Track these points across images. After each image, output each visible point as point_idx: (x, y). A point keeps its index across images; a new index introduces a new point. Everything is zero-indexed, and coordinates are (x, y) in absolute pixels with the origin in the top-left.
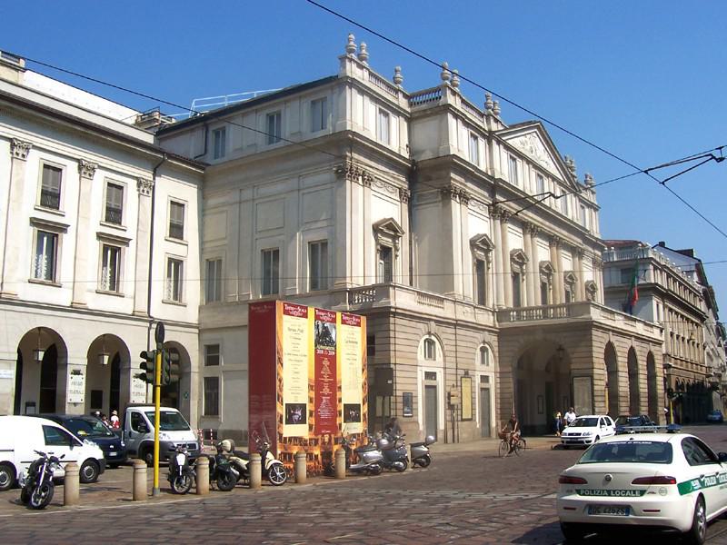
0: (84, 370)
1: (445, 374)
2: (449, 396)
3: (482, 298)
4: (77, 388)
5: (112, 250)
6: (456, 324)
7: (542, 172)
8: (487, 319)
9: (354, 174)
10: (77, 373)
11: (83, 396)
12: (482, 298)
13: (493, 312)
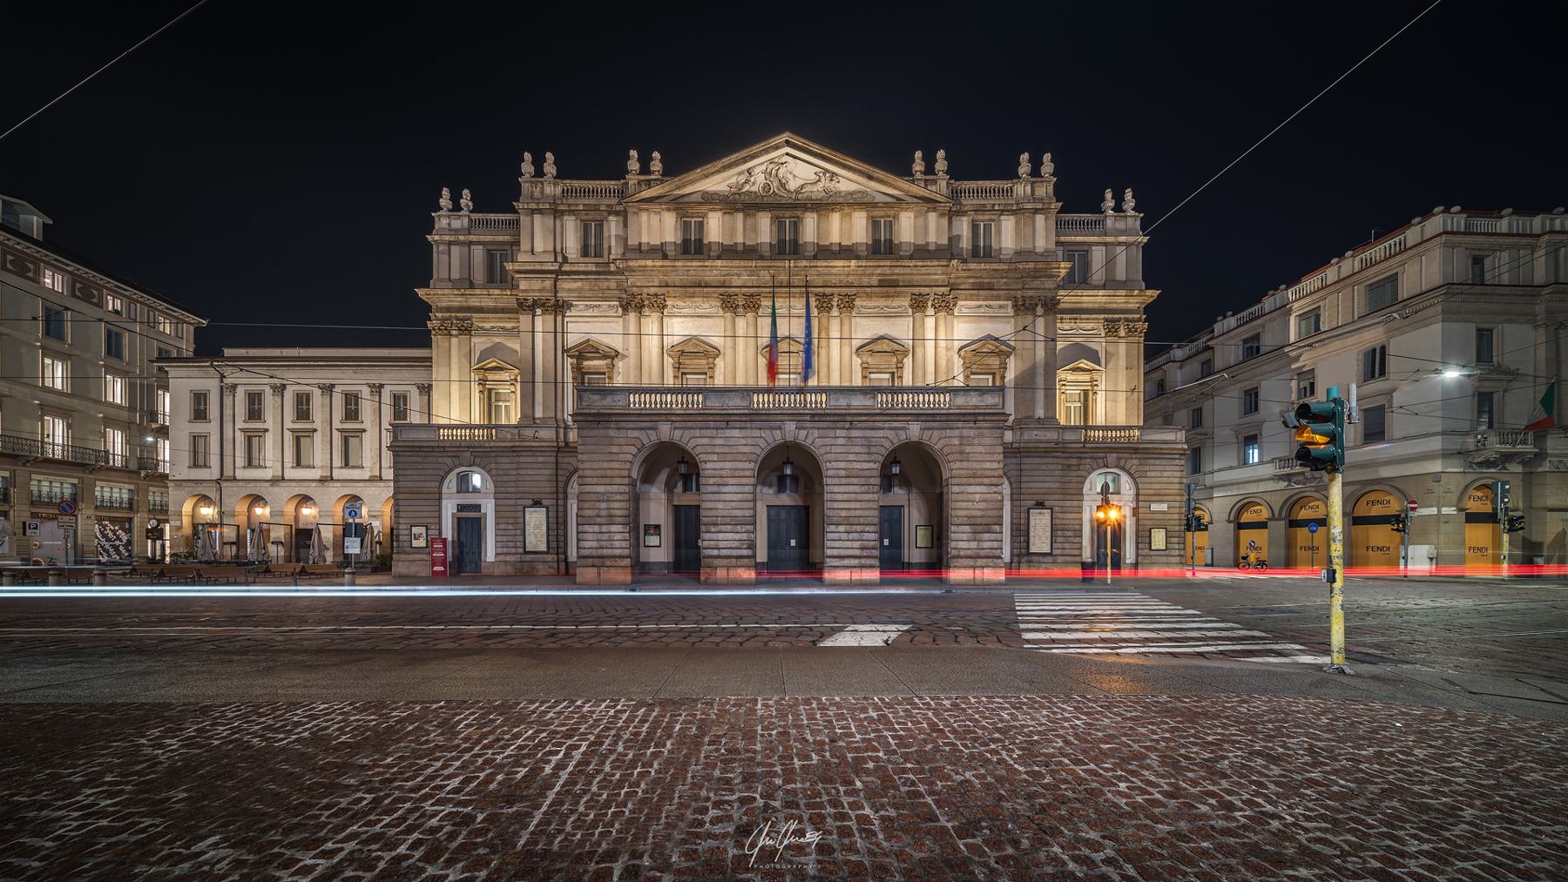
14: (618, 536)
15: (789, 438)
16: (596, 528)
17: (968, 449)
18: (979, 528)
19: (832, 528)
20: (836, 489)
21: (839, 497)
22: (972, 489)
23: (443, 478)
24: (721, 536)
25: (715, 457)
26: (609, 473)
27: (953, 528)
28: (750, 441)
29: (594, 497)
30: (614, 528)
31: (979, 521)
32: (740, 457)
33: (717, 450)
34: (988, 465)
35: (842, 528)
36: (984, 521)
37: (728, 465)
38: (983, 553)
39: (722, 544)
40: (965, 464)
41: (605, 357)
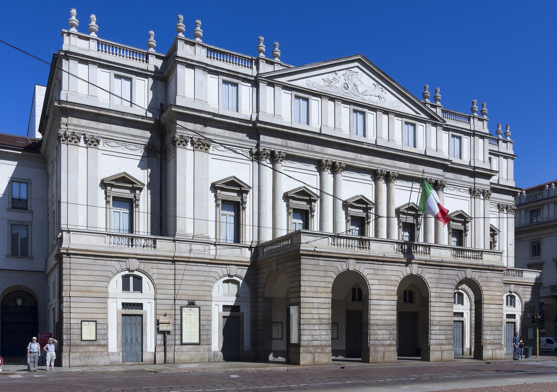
1: (156, 304)
2: (158, 323)
3: (237, 237)
12: (237, 237)
13: (250, 248)
15: (414, 273)
16: (311, 327)
17: (490, 284)
21: (436, 309)
22: (491, 306)
24: (380, 332)
25: (376, 282)
26: (320, 290)
28: (394, 273)
29: (310, 305)
30: (322, 327)
32: (389, 283)
36: (496, 324)
37: (384, 287)
40: (489, 293)
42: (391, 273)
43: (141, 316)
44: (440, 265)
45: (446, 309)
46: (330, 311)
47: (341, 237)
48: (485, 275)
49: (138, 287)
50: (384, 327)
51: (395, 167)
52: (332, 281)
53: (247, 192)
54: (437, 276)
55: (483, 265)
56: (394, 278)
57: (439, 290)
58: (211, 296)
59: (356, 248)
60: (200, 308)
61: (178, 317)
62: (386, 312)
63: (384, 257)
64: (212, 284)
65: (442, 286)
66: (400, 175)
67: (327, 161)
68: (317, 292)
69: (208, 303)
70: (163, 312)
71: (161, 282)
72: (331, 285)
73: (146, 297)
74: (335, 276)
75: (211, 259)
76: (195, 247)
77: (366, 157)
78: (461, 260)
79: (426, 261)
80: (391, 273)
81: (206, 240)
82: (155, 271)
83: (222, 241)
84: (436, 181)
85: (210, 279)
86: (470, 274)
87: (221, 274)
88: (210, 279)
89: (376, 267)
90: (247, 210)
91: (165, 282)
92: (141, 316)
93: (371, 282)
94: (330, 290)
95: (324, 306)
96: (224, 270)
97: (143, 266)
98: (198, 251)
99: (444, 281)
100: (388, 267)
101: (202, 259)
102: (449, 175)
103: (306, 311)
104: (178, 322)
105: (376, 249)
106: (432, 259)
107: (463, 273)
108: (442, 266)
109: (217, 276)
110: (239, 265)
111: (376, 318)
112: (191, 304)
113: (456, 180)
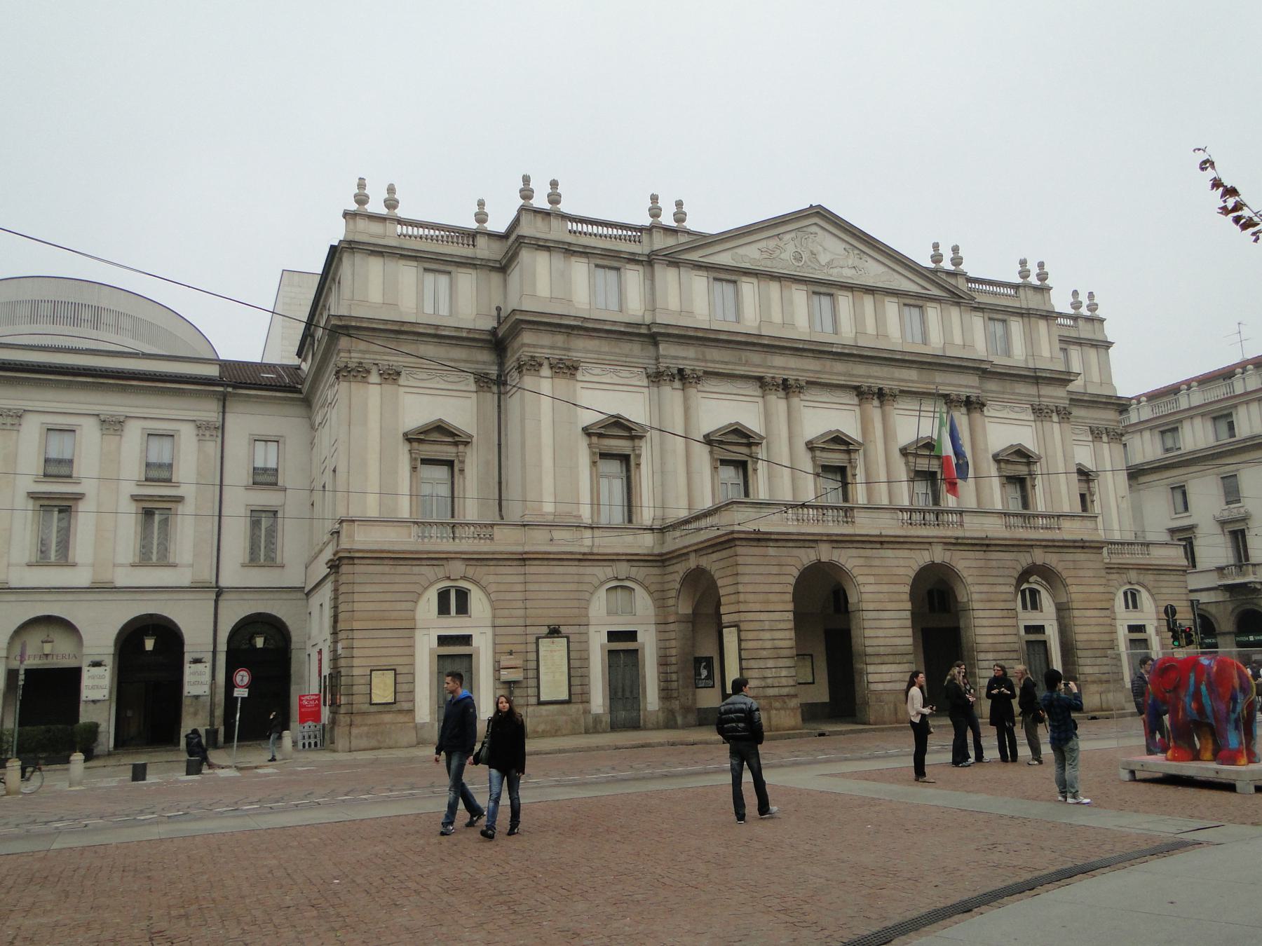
0: (109, 661)
1: (495, 635)
2: (497, 669)
4: (96, 682)
5: (154, 513)
6: (523, 559)
7: (824, 288)
8: (647, 543)
9: (358, 373)
10: (97, 664)
11: (106, 692)
14: (784, 673)
16: (761, 664)
17: (1081, 573)
18: (1098, 653)
19: (982, 656)
20: (980, 614)
21: (985, 622)
22: (1089, 613)
23: (420, 595)
24: (884, 668)
25: (871, 579)
27: (1079, 653)
28: (902, 562)
30: (781, 663)
31: (1097, 645)
33: (876, 571)
34: (1096, 589)
35: (990, 656)
36: (1100, 645)
37: (885, 588)
38: (1105, 677)
39: (886, 677)
40: (1081, 589)
41: (632, 438)
42: (895, 562)
43: (470, 656)
44: (984, 545)
45: (1003, 622)
46: (792, 634)
47: (808, 507)
48: (1069, 557)
49: (463, 609)
50: (891, 659)
51: (892, 379)
52: (793, 581)
53: (641, 437)
54: (982, 563)
55: (1064, 541)
56: (902, 571)
57: (984, 588)
58: (587, 616)
59: (831, 524)
60: (568, 638)
61: (532, 656)
62: (893, 632)
63: (881, 536)
64: (587, 596)
65: (991, 580)
66: (902, 391)
67: (773, 378)
68: (767, 602)
69: (583, 629)
70: (507, 648)
71: (502, 596)
72: (791, 589)
73: (478, 624)
74: (796, 574)
75: (584, 554)
76: (558, 534)
77: (839, 367)
78: (1022, 533)
79: (957, 538)
80: (895, 562)
81: (573, 521)
82: (492, 578)
83: (604, 521)
84: (968, 397)
85: (584, 587)
86: (1039, 557)
87: (603, 578)
88: (584, 587)
89: (868, 553)
90: (643, 467)
91: (509, 596)
92: (470, 656)
93: (861, 579)
94: (789, 597)
95: (782, 626)
96: (609, 571)
97: (470, 572)
98: (565, 541)
99: (994, 572)
100: (889, 553)
101: (571, 553)
102: (992, 386)
103: (750, 635)
104: (533, 665)
105: (865, 525)
106: (968, 534)
107: (1027, 555)
108: (988, 545)
109: (596, 582)
110: (633, 559)
111: (875, 642)
112: (554, 632)
113: (1003, 393)
